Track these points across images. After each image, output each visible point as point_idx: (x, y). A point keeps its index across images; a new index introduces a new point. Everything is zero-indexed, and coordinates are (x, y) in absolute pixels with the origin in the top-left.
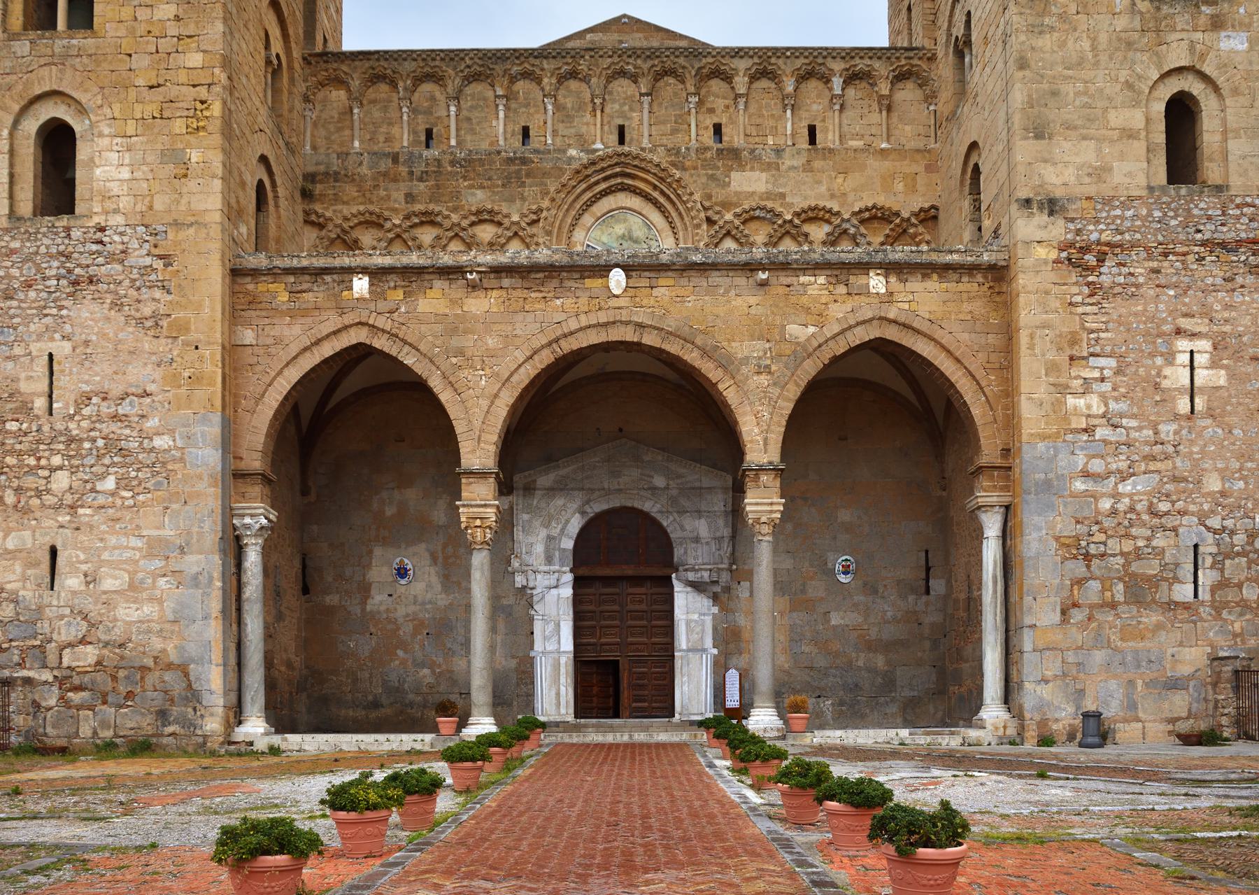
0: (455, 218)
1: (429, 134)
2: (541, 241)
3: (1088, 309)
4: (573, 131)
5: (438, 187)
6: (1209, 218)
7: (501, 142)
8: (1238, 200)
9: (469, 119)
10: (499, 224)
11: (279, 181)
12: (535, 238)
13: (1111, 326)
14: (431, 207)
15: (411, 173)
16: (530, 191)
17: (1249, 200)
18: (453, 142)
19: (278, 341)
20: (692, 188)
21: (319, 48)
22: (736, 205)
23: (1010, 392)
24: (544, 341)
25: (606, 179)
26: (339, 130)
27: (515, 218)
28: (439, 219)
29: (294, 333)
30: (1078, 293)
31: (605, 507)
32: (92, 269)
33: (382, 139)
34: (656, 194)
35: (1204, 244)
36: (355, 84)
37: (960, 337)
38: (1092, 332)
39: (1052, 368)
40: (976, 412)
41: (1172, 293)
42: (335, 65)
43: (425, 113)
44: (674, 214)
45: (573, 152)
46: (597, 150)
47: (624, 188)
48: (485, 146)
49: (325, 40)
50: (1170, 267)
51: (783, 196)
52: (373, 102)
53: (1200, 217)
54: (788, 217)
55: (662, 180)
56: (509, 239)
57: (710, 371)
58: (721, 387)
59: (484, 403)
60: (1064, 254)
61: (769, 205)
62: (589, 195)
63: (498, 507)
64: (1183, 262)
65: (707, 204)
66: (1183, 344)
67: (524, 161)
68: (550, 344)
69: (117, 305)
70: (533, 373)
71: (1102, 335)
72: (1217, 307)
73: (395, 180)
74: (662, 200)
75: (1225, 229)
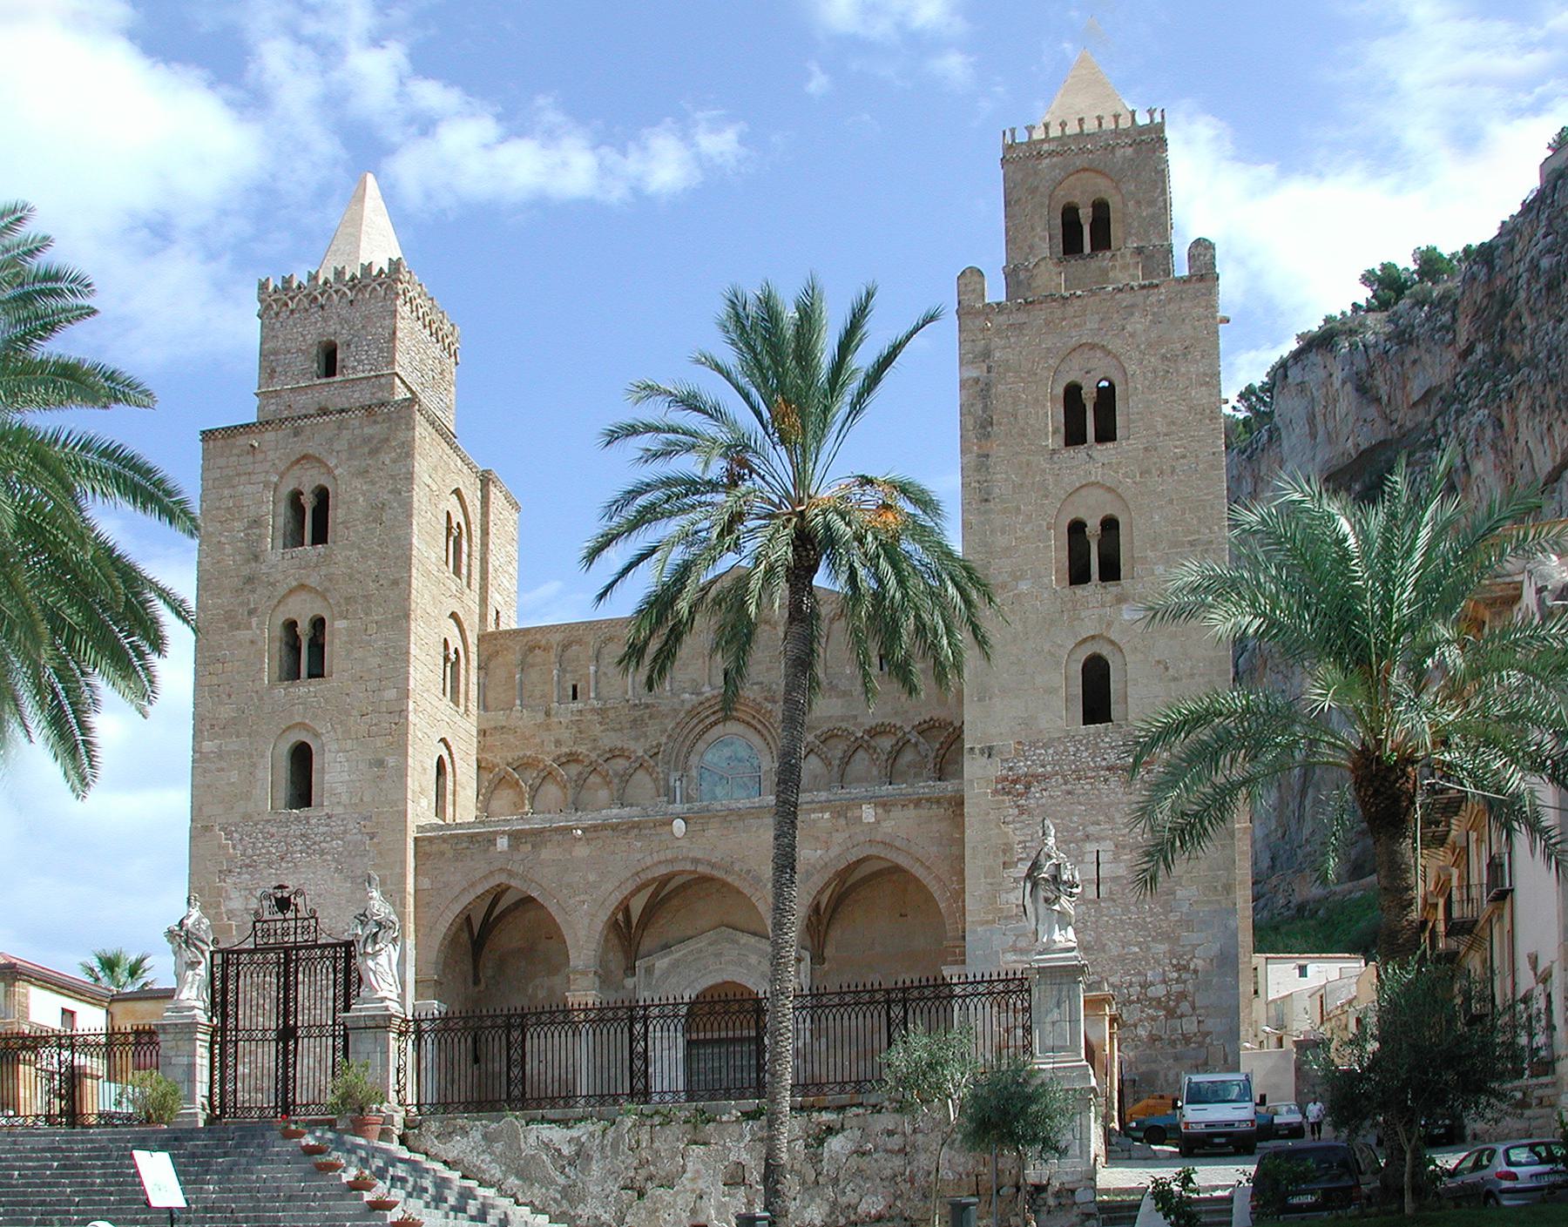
0: (593, 756)
1: (575, 688)
3: (1018, 825)
11: (453, 749)
14: (574, 750)
16: (652, 728)
18: (592, 695)
21: (491, 628)
22: (815, 728)
23: (960, 894)
25: (714, 713)
27: (640, 753)
33: (537, 693)
34: (754, 722)
43: (572, 672)
44: (769, 738)
46: (702, 693)
49: (498, 613)
51: (855, 717)
55: (758, 712)
61: (844, 725)
62: (701, 726)
66: (1091, 847)
67: (647, 706)
70: (620, 898)
73: (548, 728)
74: (759, 727)
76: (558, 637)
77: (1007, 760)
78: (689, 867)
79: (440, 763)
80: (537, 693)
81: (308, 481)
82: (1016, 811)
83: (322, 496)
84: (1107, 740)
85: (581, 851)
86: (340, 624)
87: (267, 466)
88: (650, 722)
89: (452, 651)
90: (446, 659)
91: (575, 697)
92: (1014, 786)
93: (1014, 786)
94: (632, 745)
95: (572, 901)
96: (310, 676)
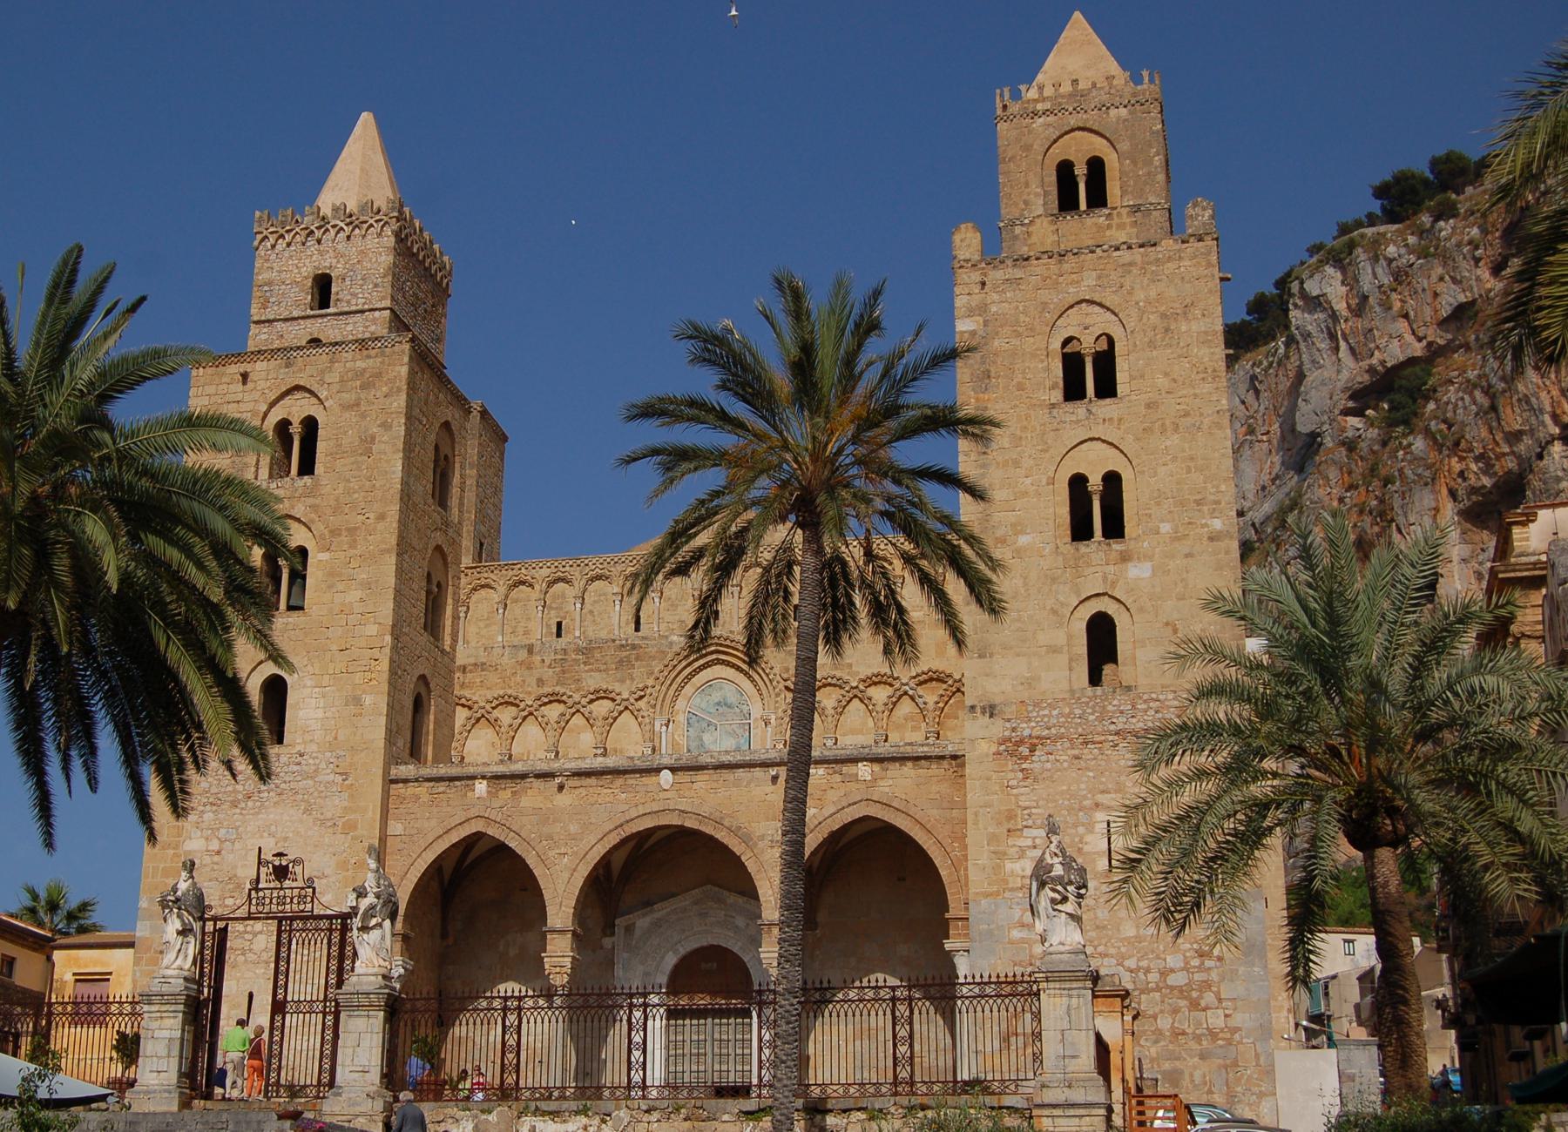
0: (577, 697)
1: (559, 625)
2: (645, 714)
4: (677, 618)
5: (564, 672)
6: (1122, 712)
7: (616, 632)
8: (1146, 697)
9: (591, 612)
10: (613, 700)
12: (642, 713)
13: (1041, 803)
14: (557, 689)
15: (543, 661)
16: (639, 671)
17: (1154, 696)
19: (419, 831)
20: (772, 662)
24: (612, 827)
26: (487, 626)
28: (564, 698)
29: (432, 827)
30: (1015, 778)
31: (696, 946)
32: (293, 785)
33: (520, 630)
35: (1117, 733)
36: (502, 589)
37: (932, 814)
38: (1025, 808)
39: (993, 838)
40: (943, 873)
41: (1091, 774)
42: (486, 575)
45: (675, 638)
47: (723, 662)
48: (603, 635)
50: (1089, 752)
52: (516, 601)
53: (1114, 712)
54: (854, 684)
56: (621, 713)
57: (736, 846)
58: (743, 859)
59: (566, 875)
60: (1003, 747)
62: (689, 670)
63: (573, 957)
64: (1100, 749)
65: (785, 676)
67: (634, 647)
68: (616, 828)
69: (307, 811)
71: (1034, 811)
72: (1129, 784)
73: (529, 668)
75: (1134, 720)
76: (545, 572)
77: (1009, 720)
78: (675, 820)
79: (419, 705)
80: (520, 630)
81: (296, 409)
82: (1020, 775)
83: (310, 425)
84: (1115, 702)
85: (564, 800)
86: (324, 556)
87: (256, 395)
88: (637, 664)
89: (435, 582)
90: (428, 592)
91: (559, 635)
92: (1017, 749)
93: (1017, 749)
94: (617, 687)
95: (551, 854)
96: (290, 608)
